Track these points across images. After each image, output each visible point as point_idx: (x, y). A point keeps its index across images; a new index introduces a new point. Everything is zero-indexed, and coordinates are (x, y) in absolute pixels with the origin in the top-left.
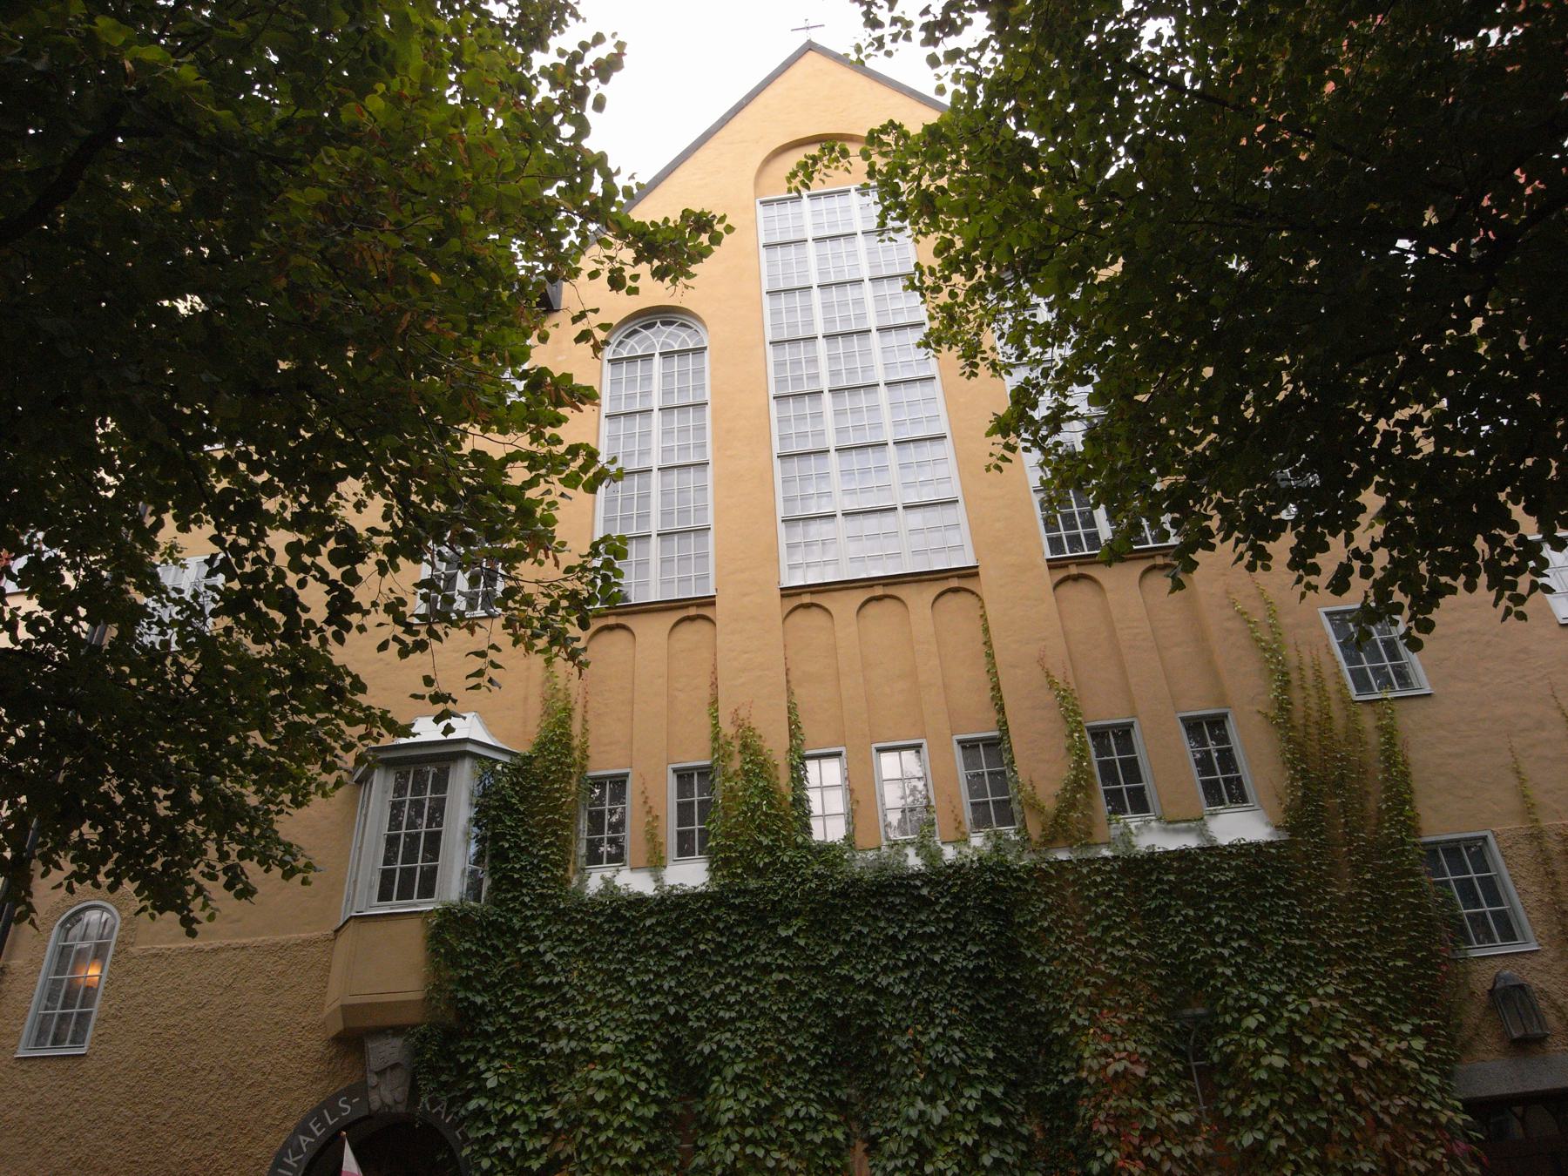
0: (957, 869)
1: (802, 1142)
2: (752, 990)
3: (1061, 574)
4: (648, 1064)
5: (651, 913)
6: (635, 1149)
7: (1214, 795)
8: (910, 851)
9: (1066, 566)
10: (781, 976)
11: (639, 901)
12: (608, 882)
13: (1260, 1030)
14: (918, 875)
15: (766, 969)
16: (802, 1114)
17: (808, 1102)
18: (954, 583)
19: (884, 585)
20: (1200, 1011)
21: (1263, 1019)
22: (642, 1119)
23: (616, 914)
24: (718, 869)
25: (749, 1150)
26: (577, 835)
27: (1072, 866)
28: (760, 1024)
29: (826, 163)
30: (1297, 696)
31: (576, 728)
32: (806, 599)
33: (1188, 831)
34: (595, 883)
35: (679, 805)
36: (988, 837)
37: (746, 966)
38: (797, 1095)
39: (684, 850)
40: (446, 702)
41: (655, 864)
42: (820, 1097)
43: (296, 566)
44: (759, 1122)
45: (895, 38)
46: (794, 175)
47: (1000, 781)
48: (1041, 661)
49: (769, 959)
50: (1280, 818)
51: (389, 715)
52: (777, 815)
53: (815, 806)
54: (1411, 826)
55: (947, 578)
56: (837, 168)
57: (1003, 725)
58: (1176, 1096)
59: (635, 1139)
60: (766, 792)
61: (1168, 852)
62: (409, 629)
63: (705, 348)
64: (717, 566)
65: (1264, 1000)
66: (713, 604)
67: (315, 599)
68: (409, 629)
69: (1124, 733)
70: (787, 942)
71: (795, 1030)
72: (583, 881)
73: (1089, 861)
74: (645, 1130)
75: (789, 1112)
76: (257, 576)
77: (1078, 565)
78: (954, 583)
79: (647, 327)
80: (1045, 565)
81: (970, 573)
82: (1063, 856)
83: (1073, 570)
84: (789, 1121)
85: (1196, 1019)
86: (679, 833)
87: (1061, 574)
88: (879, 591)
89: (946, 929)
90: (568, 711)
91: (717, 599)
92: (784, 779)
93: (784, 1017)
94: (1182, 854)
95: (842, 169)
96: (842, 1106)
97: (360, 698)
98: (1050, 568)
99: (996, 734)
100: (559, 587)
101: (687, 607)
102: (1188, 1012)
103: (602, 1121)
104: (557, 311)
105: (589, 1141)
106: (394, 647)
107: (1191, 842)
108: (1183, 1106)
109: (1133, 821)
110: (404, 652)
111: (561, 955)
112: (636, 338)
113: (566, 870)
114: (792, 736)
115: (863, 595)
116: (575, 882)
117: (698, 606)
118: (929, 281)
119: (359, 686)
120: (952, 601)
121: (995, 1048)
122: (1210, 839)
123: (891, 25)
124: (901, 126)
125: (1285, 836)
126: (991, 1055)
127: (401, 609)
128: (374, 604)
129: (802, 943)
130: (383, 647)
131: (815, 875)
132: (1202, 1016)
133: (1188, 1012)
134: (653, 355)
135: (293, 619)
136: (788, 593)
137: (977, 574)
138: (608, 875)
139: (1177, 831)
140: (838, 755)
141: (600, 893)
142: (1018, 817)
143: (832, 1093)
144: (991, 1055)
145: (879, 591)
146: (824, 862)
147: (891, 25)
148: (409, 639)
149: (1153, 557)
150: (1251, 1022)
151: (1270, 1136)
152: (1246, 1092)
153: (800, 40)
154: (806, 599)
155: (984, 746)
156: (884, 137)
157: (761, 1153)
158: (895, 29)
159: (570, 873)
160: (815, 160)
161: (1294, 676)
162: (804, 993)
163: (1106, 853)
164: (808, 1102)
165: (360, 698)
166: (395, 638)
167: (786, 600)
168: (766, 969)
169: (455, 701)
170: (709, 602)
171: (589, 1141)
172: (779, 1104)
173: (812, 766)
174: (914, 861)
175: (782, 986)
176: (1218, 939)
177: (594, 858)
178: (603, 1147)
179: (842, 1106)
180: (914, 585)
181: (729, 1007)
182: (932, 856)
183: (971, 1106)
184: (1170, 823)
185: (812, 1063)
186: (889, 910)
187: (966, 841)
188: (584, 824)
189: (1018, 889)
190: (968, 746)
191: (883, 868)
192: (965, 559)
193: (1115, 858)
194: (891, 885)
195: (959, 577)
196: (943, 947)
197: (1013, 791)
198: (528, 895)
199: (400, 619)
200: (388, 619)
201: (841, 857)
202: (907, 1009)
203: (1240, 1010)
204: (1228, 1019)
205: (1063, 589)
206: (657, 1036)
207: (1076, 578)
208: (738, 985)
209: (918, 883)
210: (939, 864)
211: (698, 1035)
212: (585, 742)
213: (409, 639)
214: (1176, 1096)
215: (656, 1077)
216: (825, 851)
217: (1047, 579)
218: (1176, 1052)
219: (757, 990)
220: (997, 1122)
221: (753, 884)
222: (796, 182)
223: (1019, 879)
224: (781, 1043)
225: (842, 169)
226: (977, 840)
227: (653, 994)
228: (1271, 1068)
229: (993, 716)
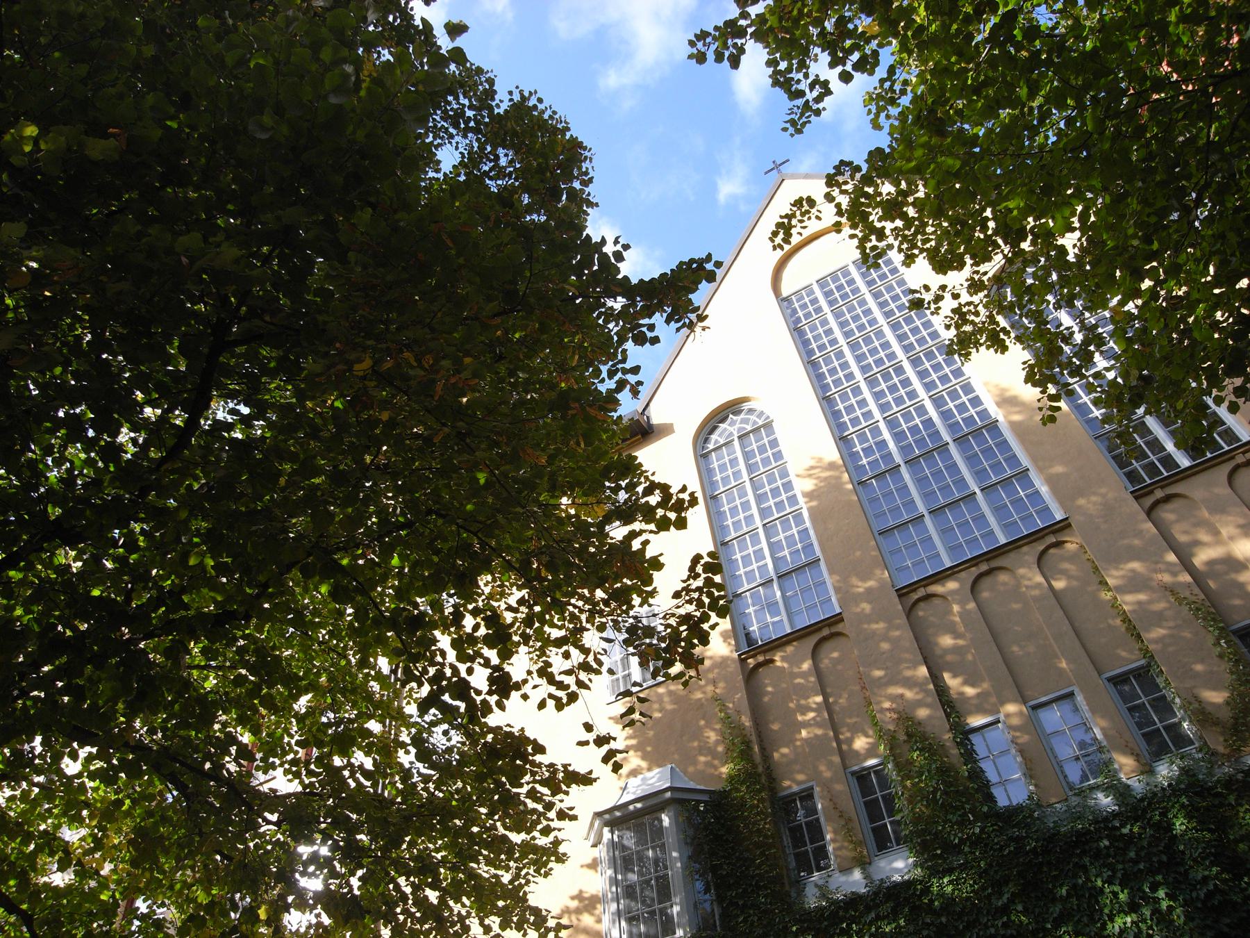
3: (1149, 501)
5: (868, 909)
9: (1152, 492)
11: (854, 901)
14: (1114, 815)
19: (987, 560)
26: (784, 852)
29: (800, 218)
31: (757, 757)
32: (921, 592)
35: (865, 803)
39: (882, 843)
40: (608, 743)
43: (462, 657)
45: (819, 99)
49: (993, 931)
51: (570, 769)
52: (957, 791)
53: (992, 775)
55: (1043, 537)
56: (809, 218)
62: (561, 686)
66: (842, 620)
67: (480, 679)
68: (561, 686)
76: (440, 675)
77: (1162, 487)
80: (1130, 498)
83: (1159, 494)
86: (874, 830)
87: (1149, 501)
89: (1160, 862)
90: (747, 744)
91: (843, 615)
95: (813, 217)
97: (538, 758)
98: (1136, 498)
99: (1143, 662)
100: (673, 615)
101: (820, 629)
106: (551, 703)
110: (560, 706)
112: (718, 432)
116: (793, 894)
117: (830, 625)
119: (540, 749)
123: (811, 91)
124: (851, 163)
127: (549, 670)
128: (529, 673)
130: (542, 705)
131: (1011, 839)
134: (733, 440)
135: (471, 703)
136: (902, 593)
137: (1069, 525)
145: (984, 567)
147: (811, 91)
148: (561, 694)
149: (1233, 458)
154: (921, 592)
156: (840, 179)
158: (815, 93)
159: (787, 888)
160: (789, 217)
165: (538, 758)
166: (551, 696)
169: (615, 739)
170: (837, 619)
173: (975, 739)
188: (787, 840)
190: (1118, 681)
195: (1054, 532)
198: (755, 914)
199: (551, 680)
200: (544, 681)
201: (1031, 816)
205: (1154, 514)
207: (1168, 499)
210: (1132, 801)
212: (768, 768)
213: (561, 694)
216: (1012, 815)
222: (778, 240)
225: (813, 217)
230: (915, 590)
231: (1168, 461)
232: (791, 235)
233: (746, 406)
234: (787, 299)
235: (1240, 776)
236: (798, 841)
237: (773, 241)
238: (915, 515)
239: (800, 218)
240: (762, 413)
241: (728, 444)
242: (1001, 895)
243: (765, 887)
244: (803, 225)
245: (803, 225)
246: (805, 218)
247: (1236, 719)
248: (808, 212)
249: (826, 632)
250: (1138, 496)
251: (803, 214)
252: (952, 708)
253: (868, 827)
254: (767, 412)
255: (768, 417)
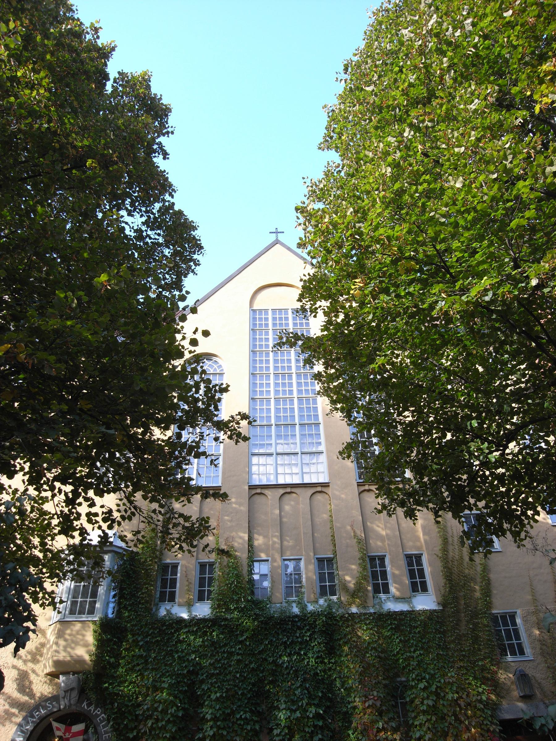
0: (313, 614)
1: (242, 729)
2: (226, 662)
3: (362, 488)
4: (181, 692)
5: (186, 626)
6: (173, 730)
7: (414, 588)
8: (294, 605)
10: (239, 657)
11: (182, 620)
12: (169, 612)
13: (425, 688)
14: (297, 616)
15: (231, 654)
16: (243, 717)
17: (245, 712)
18: (319, 489)
20: (403, 679)
21: (426, 684)
22: (177, 716)
23: (170, 626)
24: (215, 609)
25: (220, 732)
28: (228, 677)
30: (451, 548)
32: (259, 491)
34: (163, 612)
36: (326, 601)
37: (224, 652)
38: (241, 709)
39: (201, 598)
41: (189, 605)
42: (251, 710)
44: (224, 720)
47: (332, 576)
48: (352, 526)
49: (234, 650)
50: (440, 599)
54: (489, 605)
57: (335, 552)
58: (391, 715)
59: (174, 726)
60: (238, 576)
64: (223, 473)
65: (427, 677)
69: (382, 559)
70: (241, 642)
71: (242, 681)
72: (158, 609)
73: (365, 614)
74: (178, 722)
75: (238, 716)
78: (319, 489)
81: (325, 485)
84: (237, 720)
85: (401, 683)
86: (199, 591)
87: (362, 488)
92: (245, 571)
93: (238, 675)
94: (402, 613)
96: (259, 714)
99: (332, 556)
102: (399, 679)
103: (160, 717)
105: (154, 726)
108: (394, 719)
109: (383, 596)
111: (147, 642)
113: (151, 605)
114: (249, 551)
115: (282, 491)
116: (154, 610)
120: (319, 497)
121: (322, 692)
122: (414, 607)
125: (441, 608)
126: (320, 694)
129: (248, 643)
131: (255, 614)
132: (404, 681)
133: (399, 679)
136: (251, 487)
138: (168, 608)
141: (165, 616)
142: (337, 594)
143: (256, 709)
144: (320, 694)
146: (259, 609)
150: (421, 685)
151: (426, 732)
152: (418, 713)
153: (273, 237)
154: (259, 491)
157: (225, 733)
161: (450, 539)
162: (246, 665)
163: (372, 611)
164: (245, 712)
168: (231, 654)
171: (154, 726)
172: (233, 713)
173: (256, 564)
174: (296, 610)
175: (239, 661)
176: (412, 650)
177: (162, 599)
178: (160, 728)
179: (259, 714)
181: (215, 668)
182: (303, 608)
183: (311, 716)
184: (397, 599)
185: (249, 696)
186: (284, 631)
187: (317, 602)
188: (159, 584)
189: (336, 624)
190: (320, 561)
191: (283, 612)
192: (322, 479)
193: (375, 613)
194: (285, 620)
196: (305, 648)
197: (336, 582)
202: (288, 674)
203: (418, 680)
204: (413, 684)
206: (186, 680)
208: (220, 660)
209: (297, 619)
210: (305, 611)
211: (202, 682)
214: (391, 715)
215: (184, 698)
218: (393, 696)
219: (228, 662)
220: (321, 723)
221: (228, 616)
223: (336, 620)
224: (235, 686)
226: (321, 601)
227: (184, 661)
228: (428, 705)
229: (332, 548)
233: (214, 359)
234: (254, 311)
235: (347, 616)
236: (164, 586)
240: (220, 366)
242: (242, 635)
243: (143, 604)
247: (355, 592)
250: (359, 484)
252: (252, 548)
253: (197, 588)
254: (224, 367)
255: (222, 370)
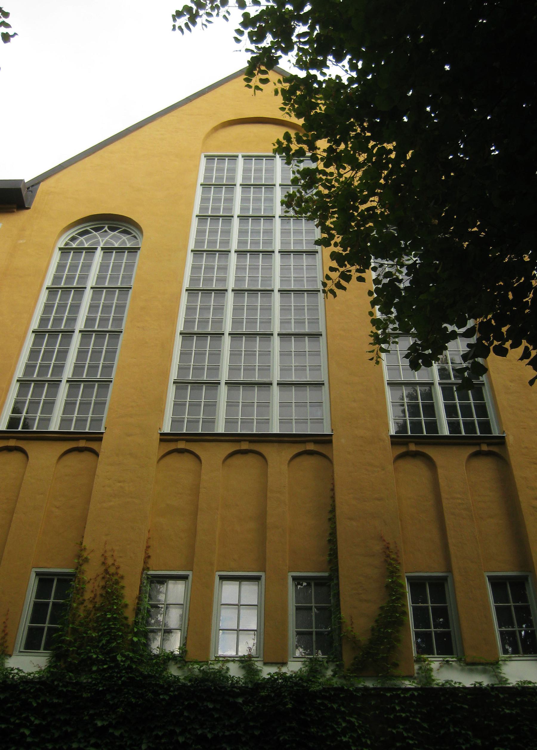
3: (401, 450)
19: (250, 442)
27: (376, 693)
33: (485, 672)
35: (36, 604)
46: (179, 14)
61: (464, 688)
63: (139, 249)
66: (100, 439)
79: (97, 230)
82: (370, 684)
87: (401, 450)
88: (245, 446)
101: (77, 439)
104: (28, 208)
107: (485, 681)
115: (230, 448)
117: (88, 440)
118: (295, 147)
134: (96, 249)
139: (471, 671)
140: (184, 578)
145: (245, 446)
155: (316, 585)
167: (164, 444)
180: (276, 444)
217: (391, 453)
230: (176, 441)
231: (433, 426)
232: (194, 23)
237: (174, 20)
238: (213, 379)
239: (209, 11)
241: (91, 250)
244: (210, 19)
245: (209, 19)
246: (214, 13)
248: (217, 7)
249: (82, 444)
251: (212, 8)
